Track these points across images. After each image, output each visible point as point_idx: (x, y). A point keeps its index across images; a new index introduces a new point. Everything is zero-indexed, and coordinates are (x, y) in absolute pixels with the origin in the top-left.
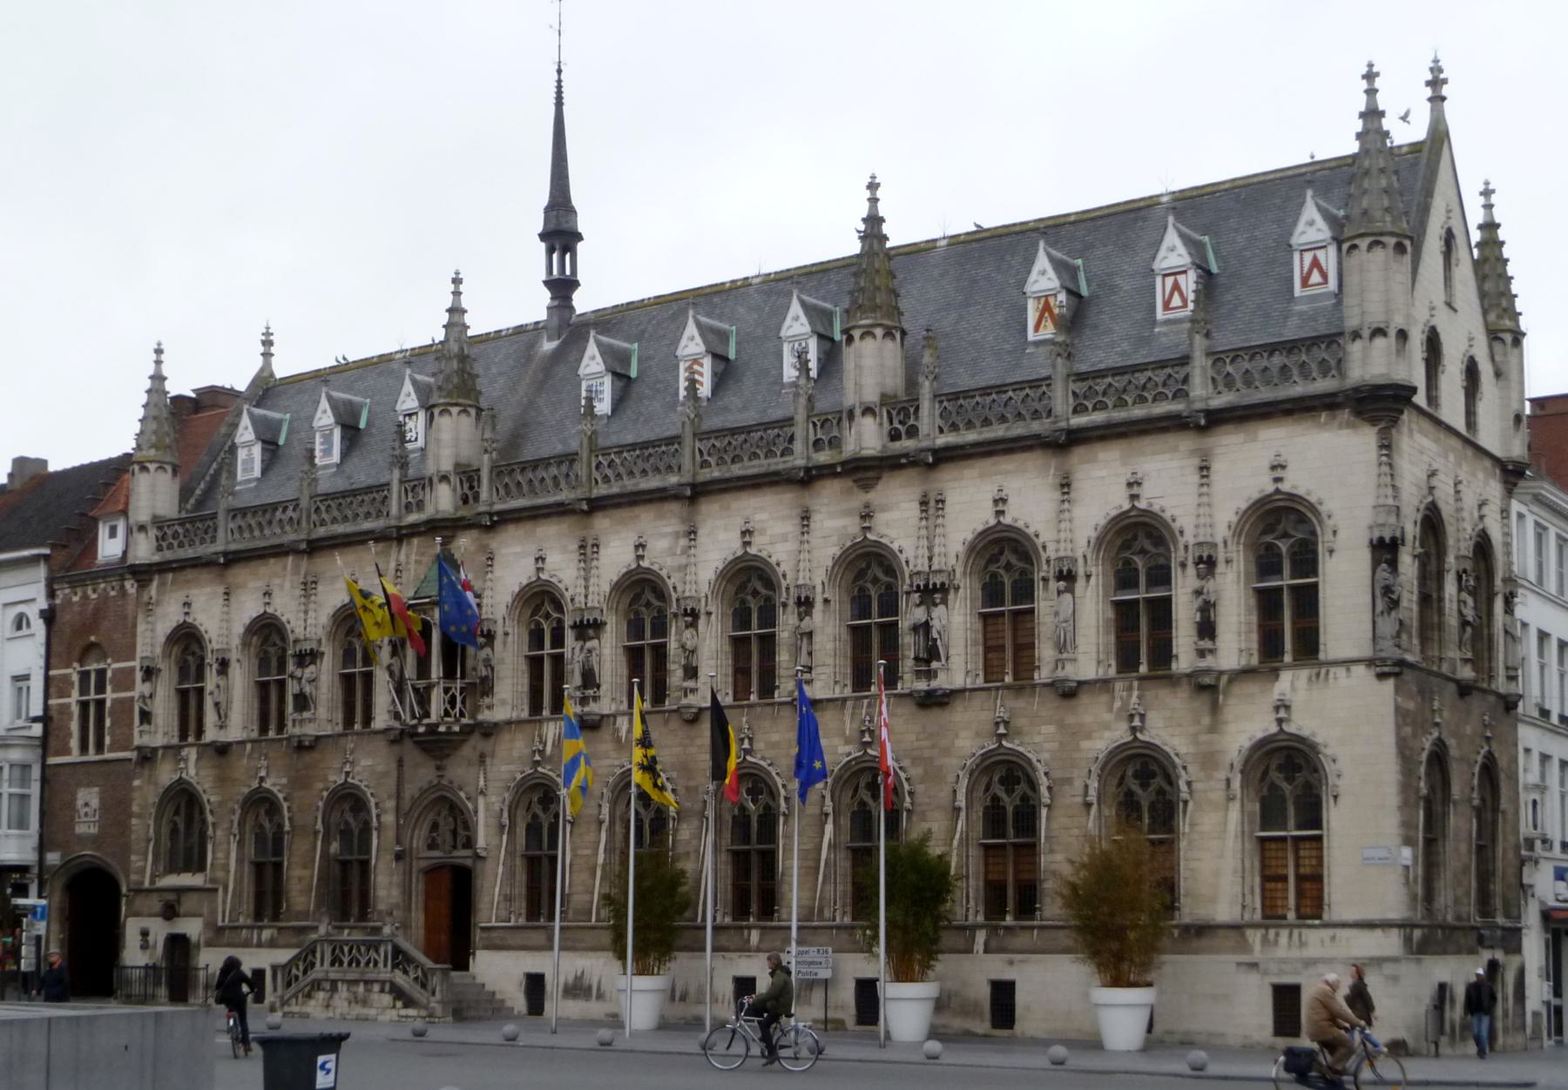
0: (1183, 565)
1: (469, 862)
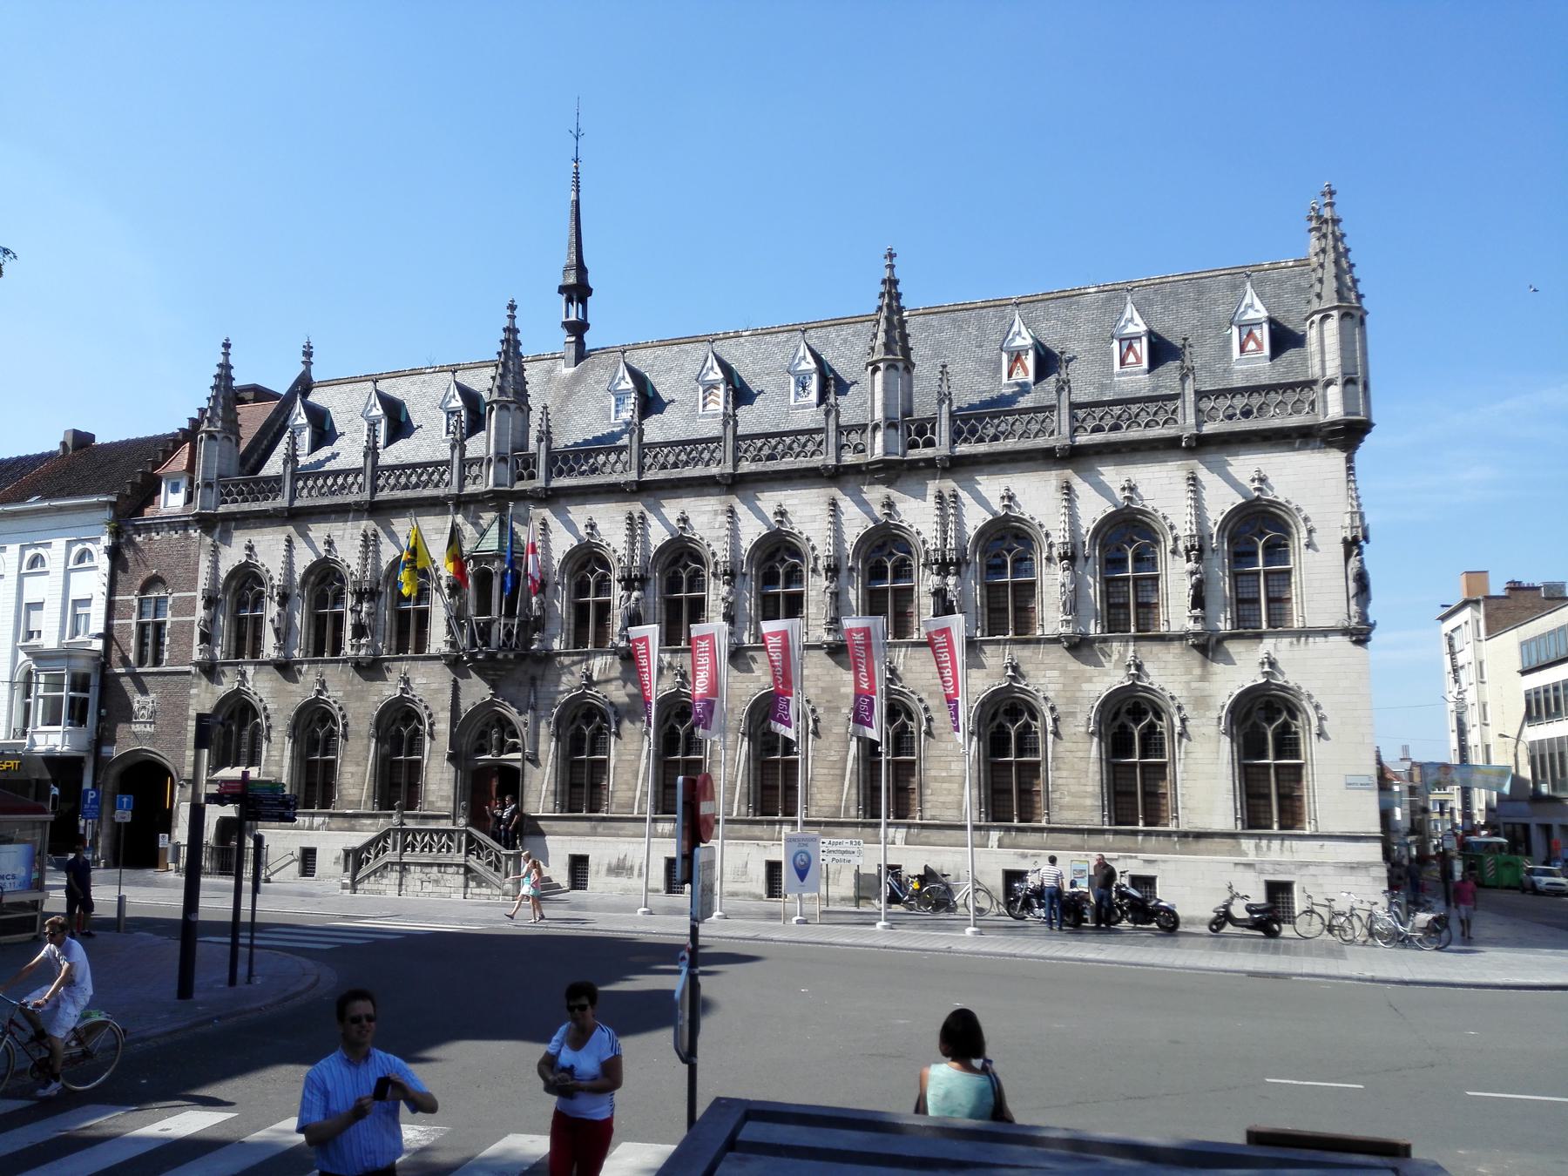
1: (518, 765)
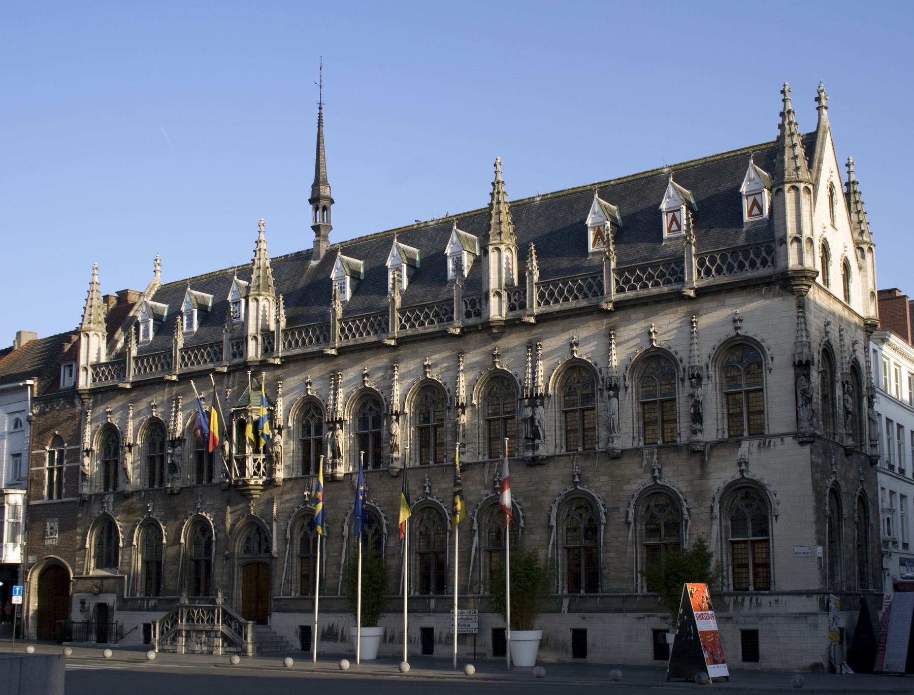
0: (683, 380)
1: (267, 560)
